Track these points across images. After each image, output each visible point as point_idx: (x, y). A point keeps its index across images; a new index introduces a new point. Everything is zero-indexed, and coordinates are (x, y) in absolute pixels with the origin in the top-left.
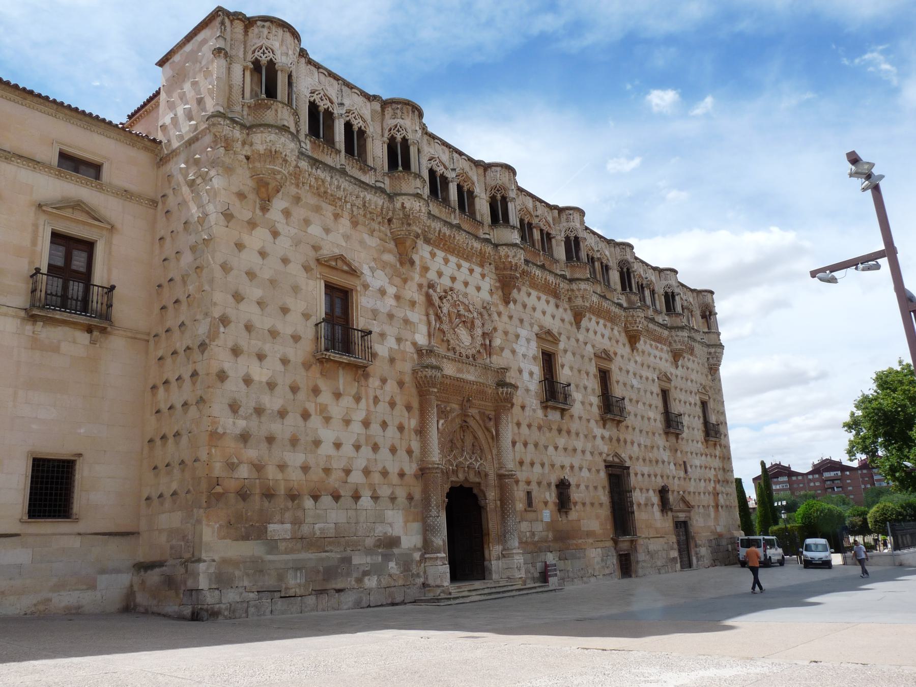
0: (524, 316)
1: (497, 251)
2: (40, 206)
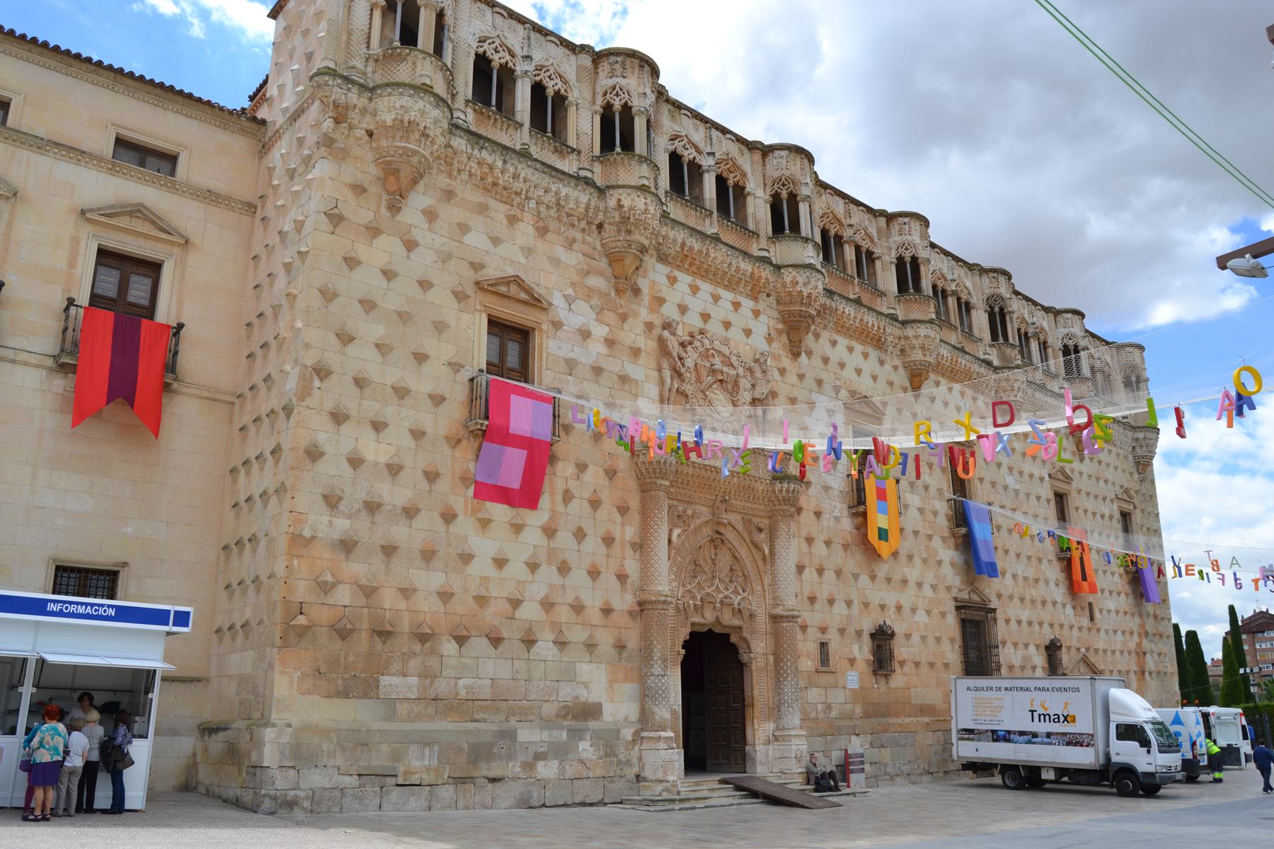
0: (824, 376)
1: (780, 276)
2: (83, 212)
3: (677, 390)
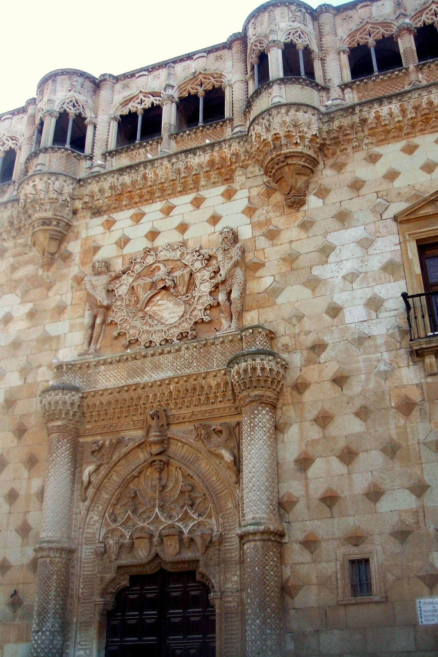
3: (103, 322)
